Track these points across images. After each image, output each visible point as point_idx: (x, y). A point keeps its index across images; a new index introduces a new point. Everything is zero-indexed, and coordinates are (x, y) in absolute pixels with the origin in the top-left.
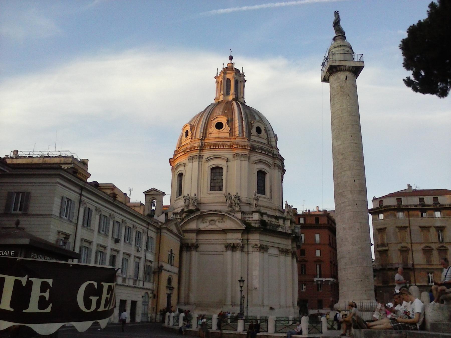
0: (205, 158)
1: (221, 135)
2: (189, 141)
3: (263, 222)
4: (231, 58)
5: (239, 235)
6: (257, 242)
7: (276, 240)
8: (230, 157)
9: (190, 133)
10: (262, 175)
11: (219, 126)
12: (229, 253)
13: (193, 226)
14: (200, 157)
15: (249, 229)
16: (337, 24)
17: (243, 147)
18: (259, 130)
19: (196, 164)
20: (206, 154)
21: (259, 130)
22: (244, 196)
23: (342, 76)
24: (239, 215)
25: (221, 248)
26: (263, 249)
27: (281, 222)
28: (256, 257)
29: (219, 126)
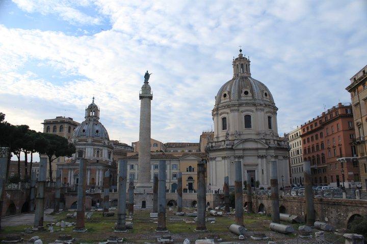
0: (240, 110)
1: (248, 98)
2: (228, 100)
4: (241, 51)
5: (265, 151)
6: (273, 154)
7: (281, 152)
8: (254, 110)
9: (228, 96)
10: (269, 118)
14: (238, 110)
15: (270, 148)
19: (236, 113)
20: (242, 109)
24: (264, 141)
26: (276, 157)
29: (246, 93)
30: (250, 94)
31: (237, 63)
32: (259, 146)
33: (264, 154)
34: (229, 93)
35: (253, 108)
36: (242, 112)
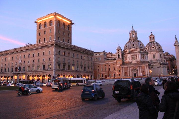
3: (163, 63)
4: (151, 32)
5: (159, 66)
7: (164, 65)
10: (161, 55)
11: (153, 47)
12: (158, 68)
13: (152, 64)
14: (151, 53)
15: (161, 64)
16: (176, 38)
17: (158, 51)
18: (160, 47)
19: (150, 54)
20: (152, 53)
21: (160, 47)
22: (159, 59)
23: (177, 46)
24: (159, 62)
25: (157, 67)
26: (163, 67)
27: (165, 63)
28: (162, 68)
29: (153, 47)
30: (154, 48)
31: (150, 37)
32: (157, 64)
33: (158, 66)
34: (148, 48)
35: (155, 52)
36: (152, 53)
